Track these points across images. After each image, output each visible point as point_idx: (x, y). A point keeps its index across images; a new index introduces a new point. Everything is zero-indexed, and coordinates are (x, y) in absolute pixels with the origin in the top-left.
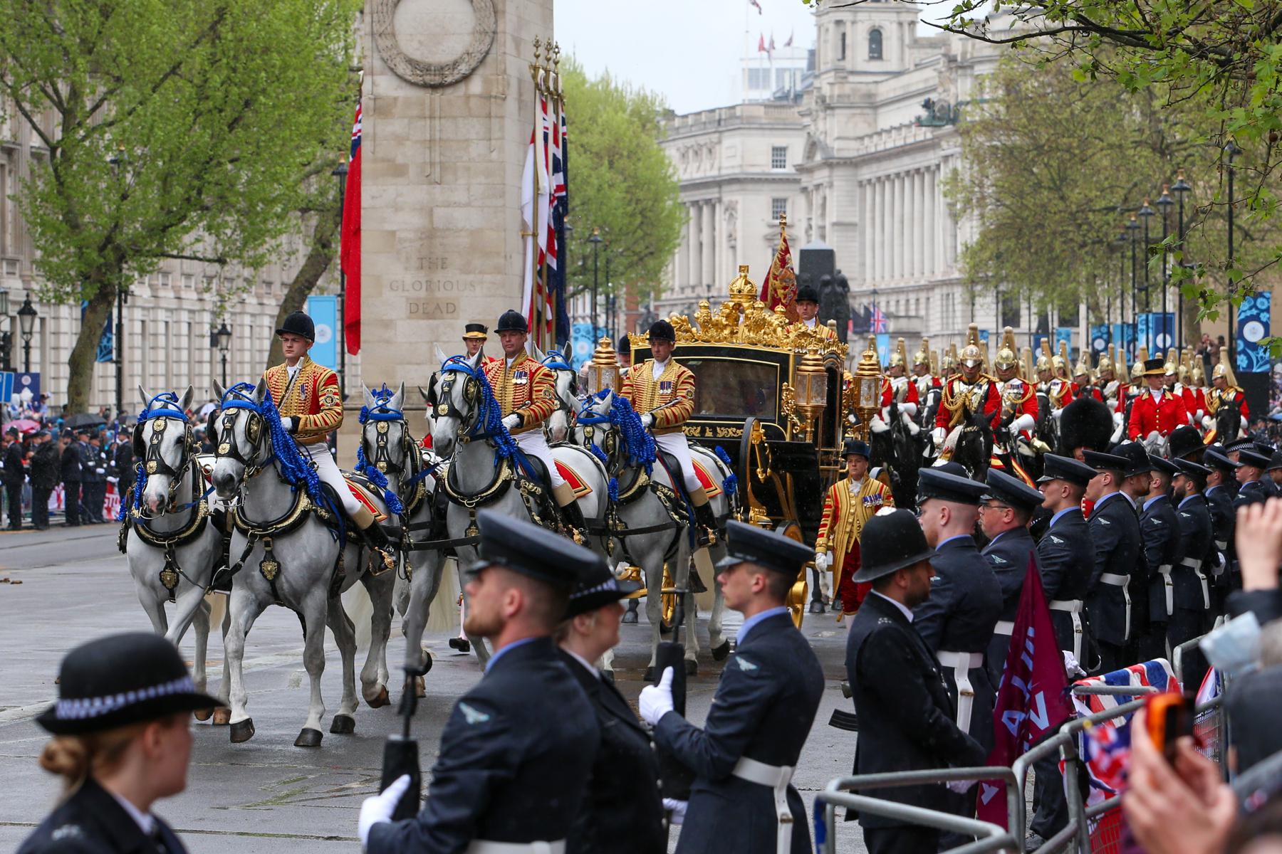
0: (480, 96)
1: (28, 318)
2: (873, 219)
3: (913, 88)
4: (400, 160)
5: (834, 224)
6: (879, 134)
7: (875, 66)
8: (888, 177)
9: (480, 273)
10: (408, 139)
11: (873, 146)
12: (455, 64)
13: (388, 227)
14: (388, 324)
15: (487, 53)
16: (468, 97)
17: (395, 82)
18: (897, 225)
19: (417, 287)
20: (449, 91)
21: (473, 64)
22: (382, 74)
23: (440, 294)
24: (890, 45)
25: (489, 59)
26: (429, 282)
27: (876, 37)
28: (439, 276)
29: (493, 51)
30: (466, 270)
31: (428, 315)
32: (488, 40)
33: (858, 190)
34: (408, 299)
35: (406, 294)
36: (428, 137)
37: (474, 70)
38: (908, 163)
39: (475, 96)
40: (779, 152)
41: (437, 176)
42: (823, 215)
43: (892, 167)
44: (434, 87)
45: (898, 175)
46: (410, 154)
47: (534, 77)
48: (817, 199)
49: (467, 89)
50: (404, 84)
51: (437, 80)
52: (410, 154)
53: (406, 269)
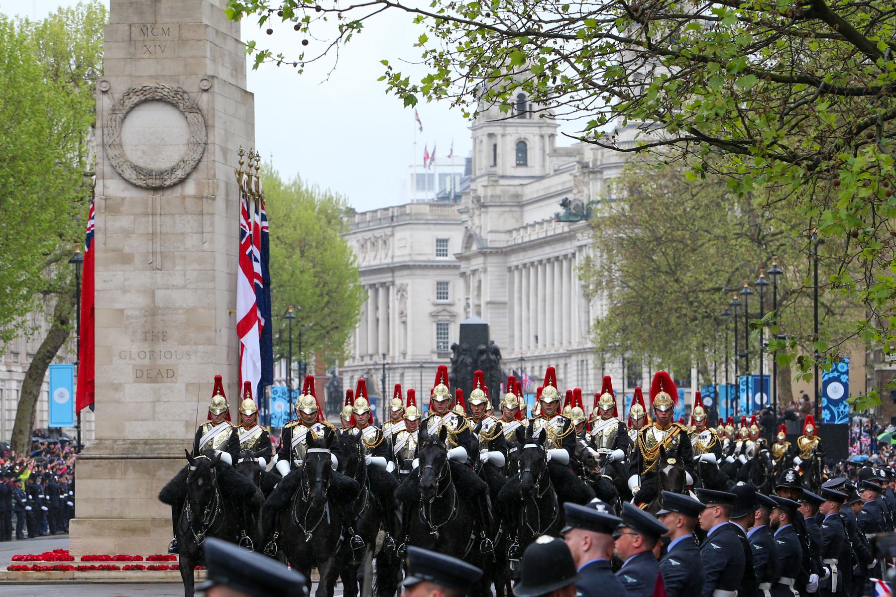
0: (195, 197)
2: (520, 298)
3: (553, 190)
4: (127, 250)
5: (488, 303)
6: (525, 228)
7: (521, 171)
8: (532, 264)
9: (195, 344)
10: (134, 233)
12: (173, 170)
13: (118, 306)
14: (117, 387)
15: (200, 160)
16: (184, 198)
17: (122, 185)
18: (540, 304)
19: (142, 356)
20: (168, 193)
21: (188, 170)
22: (112, 178)
23: (162, 362)
25: (201, 165)
26: (152, 352)
27: (522, 148)
28: (161, 347)
29: (205, 159)
30: (183, 341)
31: (153, 380)
32: (200, 150)
33: (508, 274)
34: (134, 366)
35: (133, 362)
36: (150, 231)
37: (188, 175)
39: (190, 197)
40: (442, 244)
42: (479, 295)
44: (156, 189)
45: (540, 262)
46: (136, 245)
47: (239, 181)
48: (473, 282)
49: (182, 189)
50: (130, 187)
51: (158, 183)
52: (136, 245)
53: (133, 341)
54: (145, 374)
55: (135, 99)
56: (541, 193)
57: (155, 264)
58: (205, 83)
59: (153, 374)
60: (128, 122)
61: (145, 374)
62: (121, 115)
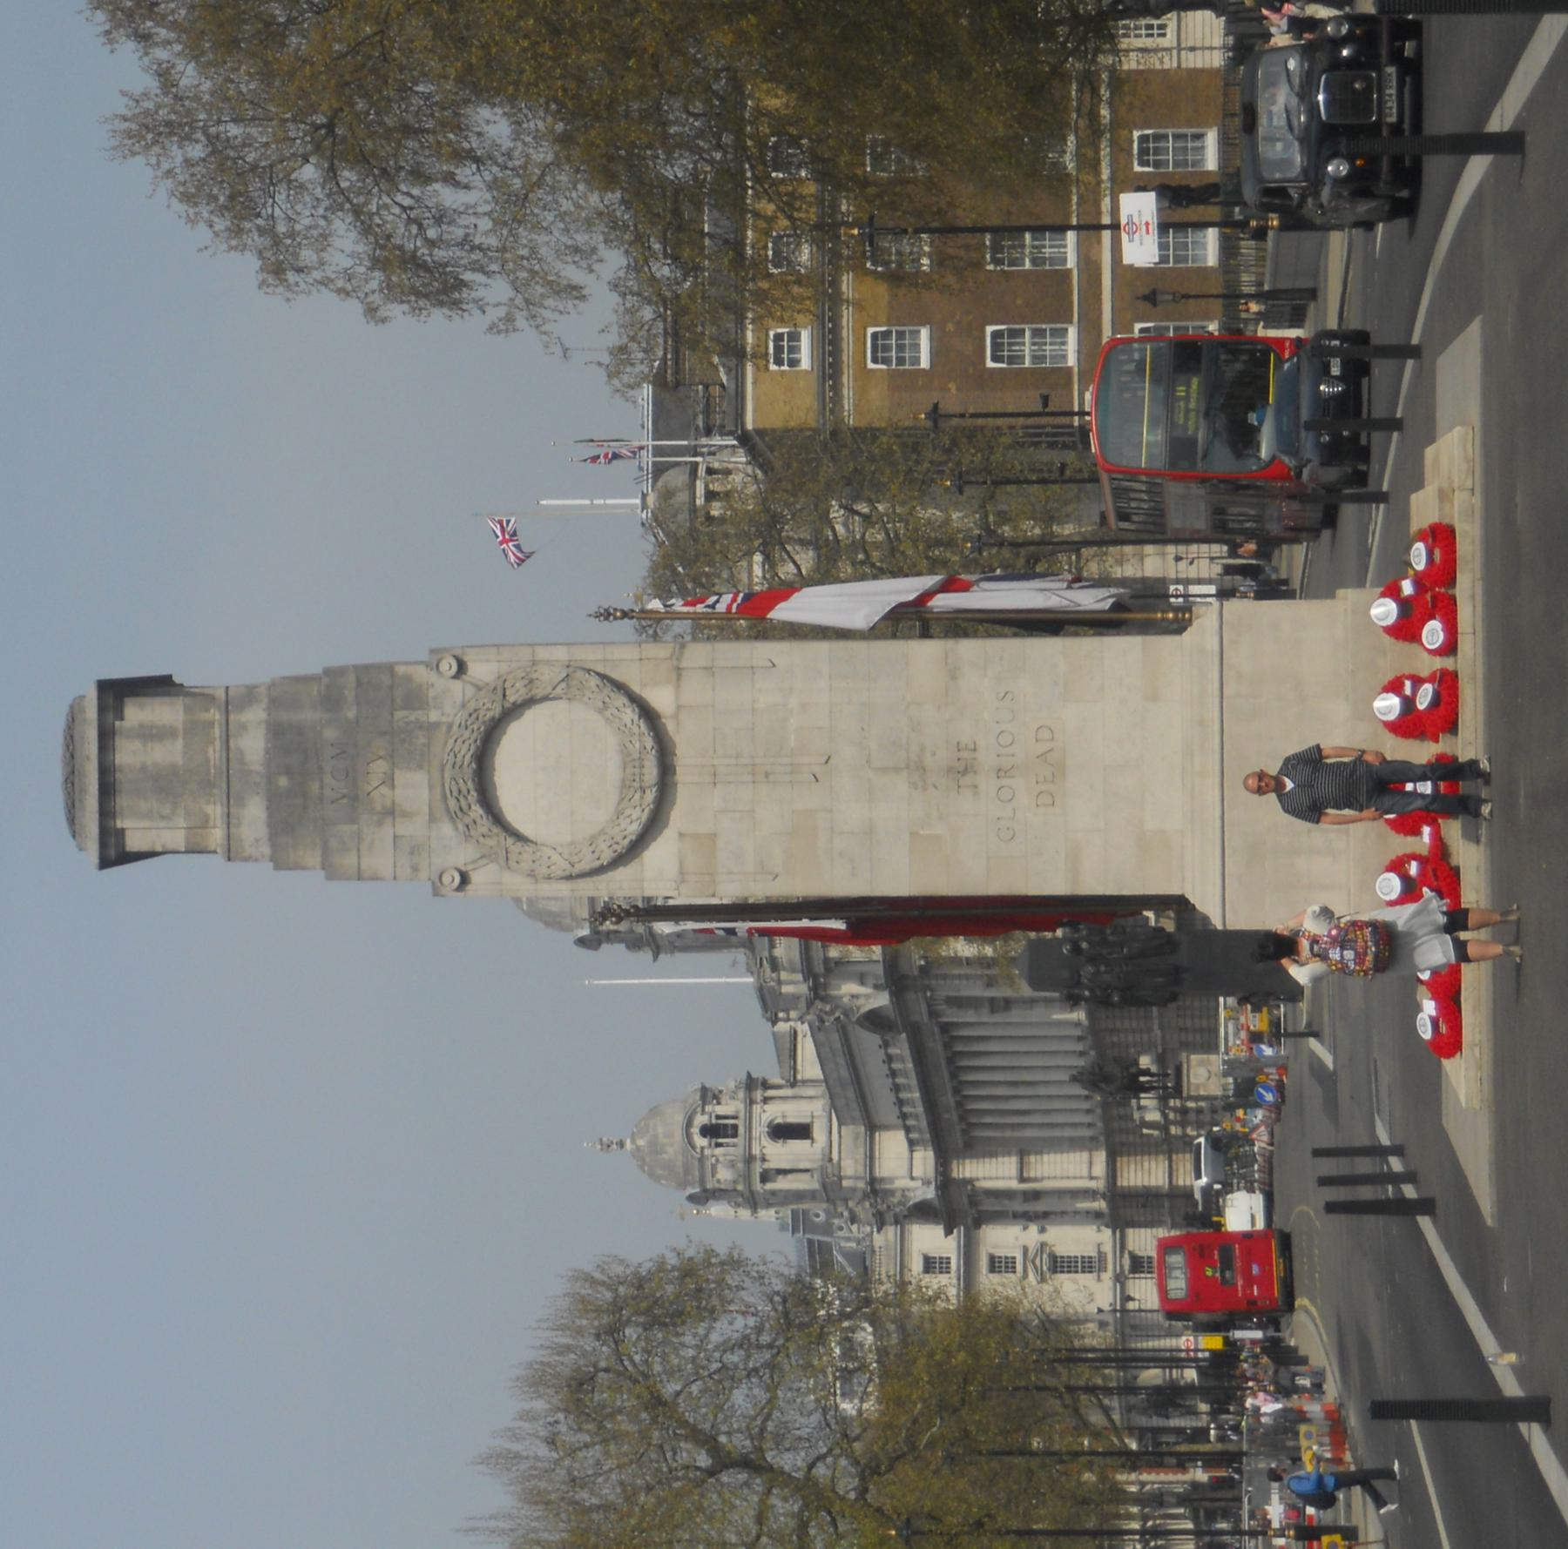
0: (678, 687)
8: (959, 1104)
15: (603, 677)
21: (620, 700)
26: (1000, 772)
29: (600, 669)
38: (943, 1078)
39: (677, 698)
43: (948, 1099)
44: (666, 769)
45: (956, 1091)
54: (1043, 787)
55: (477, 811)
57: (816, 769)
58: (444, 666)
60: (525, 829)
61: (1043, 787)
62: (510, 841)
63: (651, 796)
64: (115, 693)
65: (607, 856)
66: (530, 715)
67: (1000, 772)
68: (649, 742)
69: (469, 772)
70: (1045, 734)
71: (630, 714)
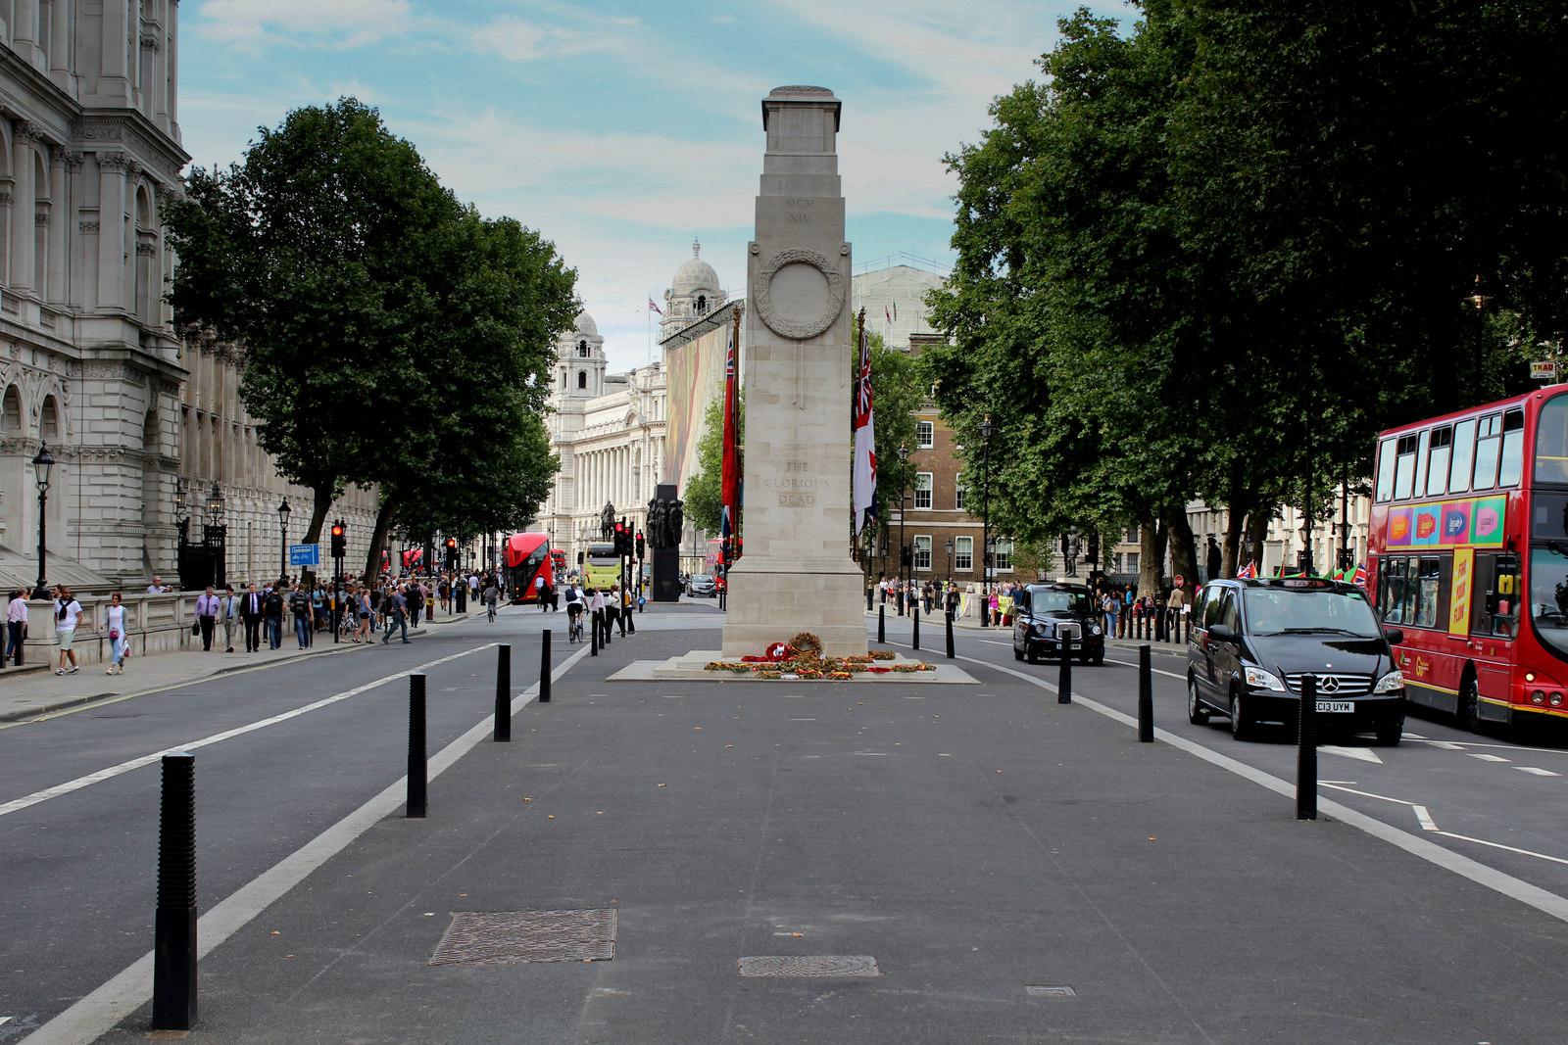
1: (284, 513)
8: (593, 452)
11: (582, 436)
14: (762, 511)
17: (769, 334)
24: (590, 381)
26: (794, 480)
27: (582, 377)
31: (794, 505)
32: (839, 305)
41: (801, 403)
43: (596, 447)
44: (799, 340)
50: (775, 337)
51: (802, 335)
56: (614, 402)
59: (795, 500)
60: (775, 280)
63: (788, 334)
64: (836, 109)
65: (763, 315)
66: (825, 282)
67: (794, 480)
68: (811, 334)
69: (798, 258)
70: (810, 500)
71: (823, 326)
